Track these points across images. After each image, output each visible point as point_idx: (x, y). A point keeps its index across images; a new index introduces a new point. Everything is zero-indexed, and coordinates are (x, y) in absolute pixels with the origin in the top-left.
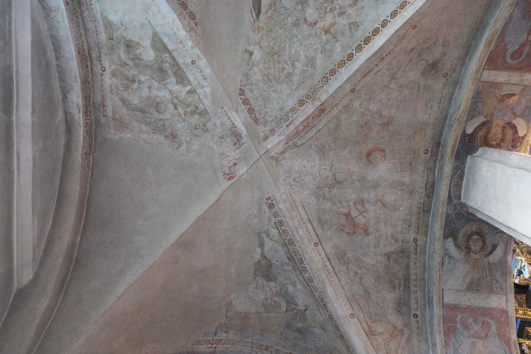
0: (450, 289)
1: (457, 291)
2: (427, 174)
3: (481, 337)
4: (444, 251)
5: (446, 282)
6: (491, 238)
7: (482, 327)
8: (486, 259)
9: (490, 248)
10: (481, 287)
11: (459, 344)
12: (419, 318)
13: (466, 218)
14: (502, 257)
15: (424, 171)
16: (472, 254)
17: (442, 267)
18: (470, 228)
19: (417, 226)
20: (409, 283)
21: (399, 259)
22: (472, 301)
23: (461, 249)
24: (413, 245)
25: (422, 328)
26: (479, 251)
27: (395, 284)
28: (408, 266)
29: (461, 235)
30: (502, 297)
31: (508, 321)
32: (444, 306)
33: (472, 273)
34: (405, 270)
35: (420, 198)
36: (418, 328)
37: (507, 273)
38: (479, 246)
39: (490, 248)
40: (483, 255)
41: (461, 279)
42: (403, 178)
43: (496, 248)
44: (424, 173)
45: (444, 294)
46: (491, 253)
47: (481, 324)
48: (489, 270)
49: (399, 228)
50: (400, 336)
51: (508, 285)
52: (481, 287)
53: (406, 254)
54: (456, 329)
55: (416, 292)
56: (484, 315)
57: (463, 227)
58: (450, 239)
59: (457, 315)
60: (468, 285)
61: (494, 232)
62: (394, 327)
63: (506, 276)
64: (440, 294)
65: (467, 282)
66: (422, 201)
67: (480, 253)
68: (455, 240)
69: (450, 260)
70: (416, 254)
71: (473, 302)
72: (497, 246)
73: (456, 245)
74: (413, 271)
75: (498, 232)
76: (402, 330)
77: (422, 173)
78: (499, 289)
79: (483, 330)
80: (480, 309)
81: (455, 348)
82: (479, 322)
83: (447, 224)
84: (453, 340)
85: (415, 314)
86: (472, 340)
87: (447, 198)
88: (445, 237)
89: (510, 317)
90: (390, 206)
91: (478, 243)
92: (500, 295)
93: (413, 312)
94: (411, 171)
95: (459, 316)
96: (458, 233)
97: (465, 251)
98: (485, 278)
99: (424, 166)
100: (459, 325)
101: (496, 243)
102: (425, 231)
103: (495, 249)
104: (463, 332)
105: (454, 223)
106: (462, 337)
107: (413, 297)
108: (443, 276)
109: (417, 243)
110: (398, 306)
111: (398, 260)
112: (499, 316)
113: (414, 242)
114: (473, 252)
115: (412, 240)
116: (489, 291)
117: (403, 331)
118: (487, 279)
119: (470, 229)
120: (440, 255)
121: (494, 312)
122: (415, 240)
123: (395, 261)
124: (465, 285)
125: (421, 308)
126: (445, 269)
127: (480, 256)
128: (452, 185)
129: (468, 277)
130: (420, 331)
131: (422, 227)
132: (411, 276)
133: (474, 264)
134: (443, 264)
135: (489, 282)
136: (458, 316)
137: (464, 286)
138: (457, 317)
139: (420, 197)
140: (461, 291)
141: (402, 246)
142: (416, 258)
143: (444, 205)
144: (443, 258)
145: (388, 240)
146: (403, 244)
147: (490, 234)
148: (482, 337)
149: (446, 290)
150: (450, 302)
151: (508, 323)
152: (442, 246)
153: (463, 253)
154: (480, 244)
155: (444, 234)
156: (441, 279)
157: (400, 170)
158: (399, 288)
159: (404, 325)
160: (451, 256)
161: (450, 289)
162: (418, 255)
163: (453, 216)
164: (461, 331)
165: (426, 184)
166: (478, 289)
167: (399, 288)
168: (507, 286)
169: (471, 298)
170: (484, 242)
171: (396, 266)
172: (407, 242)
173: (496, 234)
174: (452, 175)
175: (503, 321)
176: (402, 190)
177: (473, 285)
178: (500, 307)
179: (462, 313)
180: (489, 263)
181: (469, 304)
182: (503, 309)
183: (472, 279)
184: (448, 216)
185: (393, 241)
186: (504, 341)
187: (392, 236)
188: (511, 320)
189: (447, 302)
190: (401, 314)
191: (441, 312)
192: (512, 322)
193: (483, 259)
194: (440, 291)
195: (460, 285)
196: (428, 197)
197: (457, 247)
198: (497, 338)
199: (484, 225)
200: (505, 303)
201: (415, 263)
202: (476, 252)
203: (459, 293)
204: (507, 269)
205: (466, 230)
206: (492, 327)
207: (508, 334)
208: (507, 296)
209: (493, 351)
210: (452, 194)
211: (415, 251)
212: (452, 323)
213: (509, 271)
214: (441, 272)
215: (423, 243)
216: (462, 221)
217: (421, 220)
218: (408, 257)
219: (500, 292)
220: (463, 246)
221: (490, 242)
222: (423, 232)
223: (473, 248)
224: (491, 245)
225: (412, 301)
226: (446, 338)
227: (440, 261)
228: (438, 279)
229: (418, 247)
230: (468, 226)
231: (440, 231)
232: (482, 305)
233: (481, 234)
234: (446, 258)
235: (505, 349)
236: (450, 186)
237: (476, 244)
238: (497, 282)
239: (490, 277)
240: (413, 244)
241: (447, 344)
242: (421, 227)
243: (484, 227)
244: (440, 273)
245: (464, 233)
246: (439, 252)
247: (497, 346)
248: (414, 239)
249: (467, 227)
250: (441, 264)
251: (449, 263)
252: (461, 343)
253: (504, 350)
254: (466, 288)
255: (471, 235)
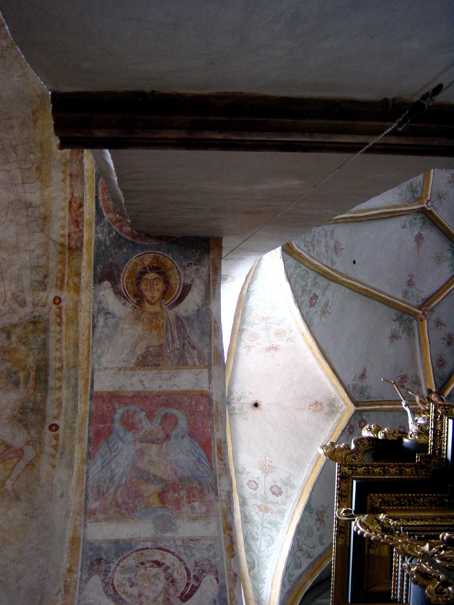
0: (106, 368)
1: (120, 370)
2: (71, 186)
3: (156, 441)
4: (96, 306)
5: (100, 357)
6: (180, 275)
7: (160, 424)
8: (171, 312)
9: (178, 293)
10: (163, 360)
11: (114, 454)
12: (60, 431)
13: (131, 245)
14: (200, 304)
15: (64, 180)
16: (147, 305)
17: (93, 333)
18: (140, 260)
19: (59, 275)
20: (47, 375)
21: (28, 335)
22: (145, 383)
23: (126, 299)
24: (55, 309)
25: (64, 446)
26: (159, 299)
27: (19, 378)
28: (45, 345)
29: (125, 275)
30: (200, 372)
31: (210, 410)
32: (95, 397)
33: (148, 337)
34: (40, 352)
35: (63, 227)
36: (55, 447)
37: (211, 331)
38: (158, 290)
39: (178, 293)
40: (166, 305)
41: (127, 351)
42: (28, 195)
43: (189, 290)
44: (65, 183)
45: (95, 378)
46: (180, 300)
47: (160, 419)
48: (179, 329)
49: (26, 282)
50: (15, 460)
51: (212, 352)
52: (163, 360)
53: (40, 326)
54: (110, 432)
55: (60, 388)
56: (168, 404)
57: (127, 261)
58: (107, 284)
59: (116, 409)
60: (140, 358)
61: (184, 264)
62: (6, 446)
63: (210, 337)
64: (88, 379)
65: (139, 353)
66: (66, 232)
67: (160, 303)
68: (115, 283)
69: (106, 319)
70: (60, 324)
71: (146, 384)
72: (190, 287)
73: (118, 293)
74: (53, 354)
75: (191, 264)
76: (21, 450)
77: (62, 183)
78: (196, 359)
79: (163, 429)
80: (159, 396)
81: (105, 460)
82: (156, 417)
83: (98, 258)
84: (103, 448)
85: (52, 425)
86: (139, 446)
87: (94, 214)
88: (97, 280)
89: (214, 403)
90: (7, 245)
91: (157, 285)
92: (198, 368)
93: (50, 421)
94: (42, 181)
95: (120, 411)
96: (120, 271)
97: (133, 302)
98: (170, 344)
99: (64, 172)
100: (117, 426)
101: (188, 281)
102: (75, 284)
103: (188, 293)
104: (125, 435)
105: (111, 255)
106: (121, 443)
107: (51, 398)
108: (95, 348)
109: (60, 305)
110: (21, 414)
111: (27, 337)
112: (194, 403)
113: (55, 303)
114: (149, 302)
115: (52, 301)
116: (177, 363)
117: (23, 452)
118: (175, 345)
119: (138, 262)
120: (90, 313)
121: (186, 398)
122: (57, 301)
123: (20, 338)
124: (135, 358)
125: (66, 414)
126: (97, 335)
127: (161, 306)
128: (100, 189)
129: (139, 346)
130: (59, 451)
131: (69, 278)
132: (50, 362)
133: (151, 322)
134: (94, 327)
135: (178, 349)
136: (118, 411)
137: (133, 361)
138: (115, 413)
139: (61, 226)
140: (126, 369)
141: (32, 312)
142: (60, 332)
143: (90, 226)
144: (94, 317)
145: (6, 304)
146: (34, 309)
147: (177, 268)
148: (158, 439)
149: (99, 370)
150: (106, 389)
151: (210, 414)
152: (92, 297)
153: (131, 305)
154: (161, 286)
155: (95, 275)
156: (91, 354)
157: (21, 182)
158: (26, 384)
159: (28, 443)
160: (108, 313)
161: (106, 368)
162: (64, 327)
163: (108, 243)
164: (122, 434)
165: (70, 202)
166: (157, 363)
167: (26, 384)
168: (211, 353)
169: (143, 378)
170: (167, 282)
171: (23, 347)
172: (41, 305)
173: (187, 268)
174: (97, 172)
175: (201, 411)
176: (27, 215)
177: (149, 357)
178: (197, 388)
179: (126, 404)
180: (178, 318)
181: (140, 390)
182: (202, 391)
183: (148, 347)
184: (99, 243)
185: (16, 306)
186: (200, 443)
187: (15, 297)
188: (217, 408)
189: (99, 390)
190: (26, 426)
191: (88, 408)
192: (218, 411)
193: (167, 313)
194: (88, 372)
195: (124, 359)
196: (75, 224)
197: (119, 296)
198: (187, 440)
199: (165, 254)
200: (208, 382)
201: (59, 341)
202: (153, 301)
203: (122, 372)
204: (211, 325)
205: (133, 266)
206: (180, 423)
207: (209, 430)
208: (210, 369)
209: (176, 460)
210: (101, 204)
211: (59, 320)
212: (105, 423)
213: (215, 327)
214: (91, 342)
215: (71, 304)
216: (125, 250)
217: (67, 264)
218: (46, 331)
219: (198, 364)
220: (129, 292)
221: (178, 282)
222: (71, 285)
223: (148, 294)
224: (180, 285)
225: (48, 402)
226: (92, 447)
227: (90, 323)
228: (86, 354)
229: (63, 312)
230: (136, 258)
231: (88, 272)
232: (164, 388)
233: (160, 269)
234: (99, 316)
235: (199, 454)
236: (97, 192)
237: (153, 288)
238: (194, 348)
239: (180, 341)
240: (55, 306)
241: (92, 456)
242: (66, 278)
243: (165, 256)
244: (89, 343)
245: (129, 271)
246: (88, 308)
247: (184, 450)
248: (56, 298)
249: (134, 261)
250: (91, 328)
251: (106, 325)
252: (116, 453)
253: (198, 456)
254: (136, 364)
255: (143, 273)
